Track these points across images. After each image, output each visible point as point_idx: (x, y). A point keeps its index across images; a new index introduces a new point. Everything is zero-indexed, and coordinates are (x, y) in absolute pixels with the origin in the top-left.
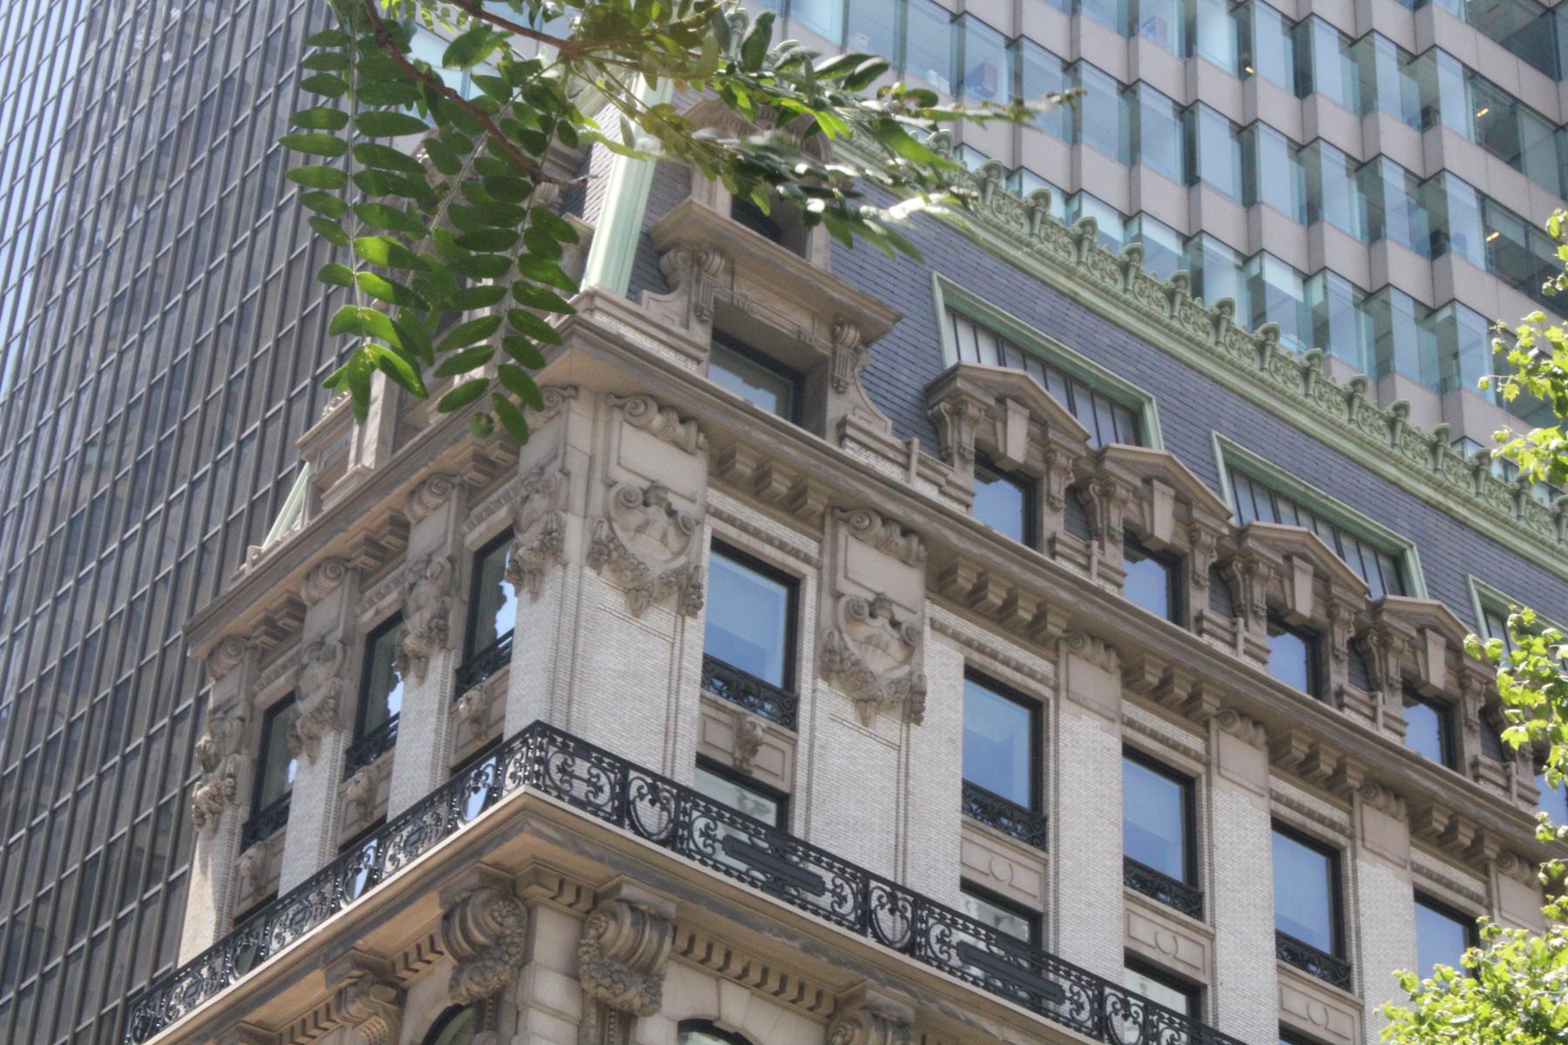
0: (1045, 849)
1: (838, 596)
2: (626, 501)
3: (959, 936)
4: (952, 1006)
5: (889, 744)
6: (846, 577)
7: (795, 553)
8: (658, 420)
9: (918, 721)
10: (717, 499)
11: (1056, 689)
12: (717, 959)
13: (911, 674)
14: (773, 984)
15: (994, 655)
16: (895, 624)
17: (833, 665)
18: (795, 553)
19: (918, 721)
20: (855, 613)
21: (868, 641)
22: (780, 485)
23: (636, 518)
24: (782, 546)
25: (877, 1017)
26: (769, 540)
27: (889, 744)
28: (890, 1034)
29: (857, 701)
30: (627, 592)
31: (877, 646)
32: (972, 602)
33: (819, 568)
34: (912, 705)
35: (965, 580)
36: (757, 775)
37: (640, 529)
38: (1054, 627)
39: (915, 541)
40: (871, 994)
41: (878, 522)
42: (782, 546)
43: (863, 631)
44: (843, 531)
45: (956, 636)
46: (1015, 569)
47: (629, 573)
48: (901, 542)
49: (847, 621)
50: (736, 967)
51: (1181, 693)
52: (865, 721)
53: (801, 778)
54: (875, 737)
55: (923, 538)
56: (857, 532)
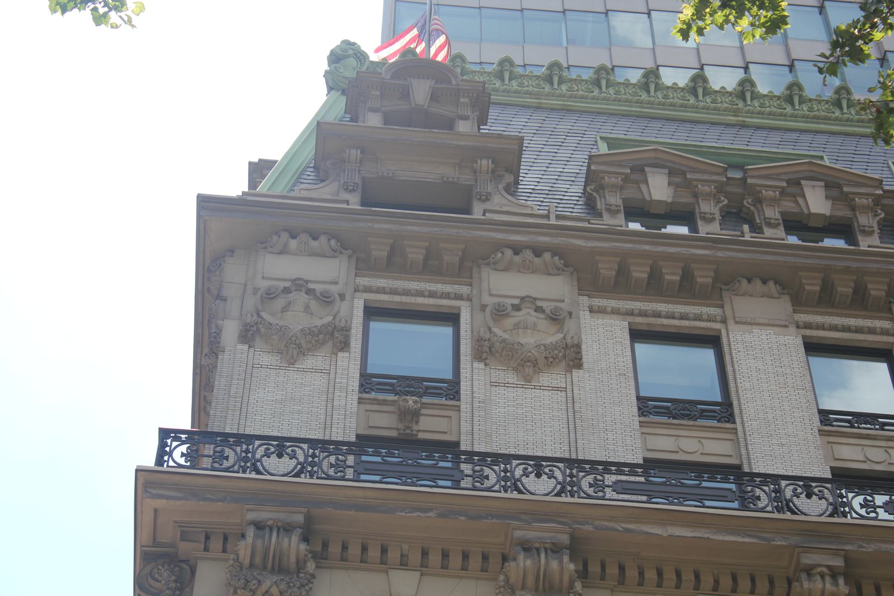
0: (734, 422)
1: (483, 307)
2: (270, 296)
3: (610, 479)
4: (606, 524)
5: (557, 389)
6: (491, 295)
7: (447, 296)
8: (293, 244)
9: (579, 366)
10: (364, 281)
11: (724, 321)
12: (374, 553)
13: (564, 338)
14: (435, 558)
15: (658, 315)
16: (539, 310)
17: (485, 351)
18: (447, 296)
19: (579, 366)
20: (500, 313)
21: (517, 326)
22: (416, 255)
23: (280, 303)
24: (432, 295)
25: (527, 548)
26: (419, 293)
27: (557, 389)
28: (543, 555)
29: (516, 370)
30: (280, 352)
31: (526, 328)
32: (621, 284)
33: (469, 299)
34: (571, 357)
35: (607, 270)
36: (421, 436)
37: (284, 310)
38: (703, 278)
39: (547, 256)
40: (518, 534)
41: (509, 253)
42: (432, 295)
43: (509, 322)
44: (485, 272)
45: (615, 312)
46: (647, 247)
47: (275, 337)
48: (537, 260)
49: (495, 320)
50: (393, 555)
51: (845, 289)
52: (528, 379)
53: (465, 427)
54: (541, 388)
55: (556, 251)
56: (495, 266)
